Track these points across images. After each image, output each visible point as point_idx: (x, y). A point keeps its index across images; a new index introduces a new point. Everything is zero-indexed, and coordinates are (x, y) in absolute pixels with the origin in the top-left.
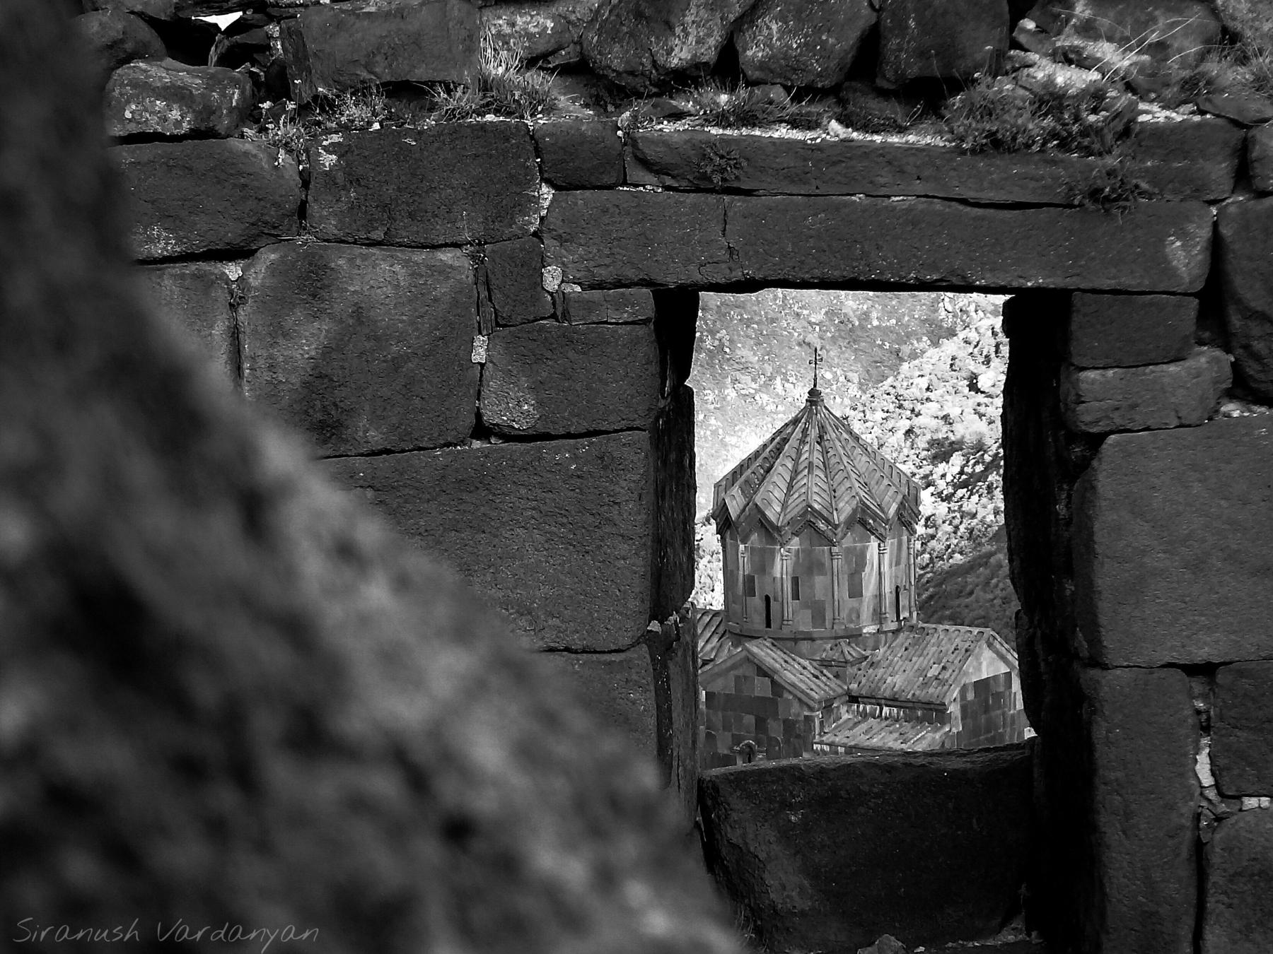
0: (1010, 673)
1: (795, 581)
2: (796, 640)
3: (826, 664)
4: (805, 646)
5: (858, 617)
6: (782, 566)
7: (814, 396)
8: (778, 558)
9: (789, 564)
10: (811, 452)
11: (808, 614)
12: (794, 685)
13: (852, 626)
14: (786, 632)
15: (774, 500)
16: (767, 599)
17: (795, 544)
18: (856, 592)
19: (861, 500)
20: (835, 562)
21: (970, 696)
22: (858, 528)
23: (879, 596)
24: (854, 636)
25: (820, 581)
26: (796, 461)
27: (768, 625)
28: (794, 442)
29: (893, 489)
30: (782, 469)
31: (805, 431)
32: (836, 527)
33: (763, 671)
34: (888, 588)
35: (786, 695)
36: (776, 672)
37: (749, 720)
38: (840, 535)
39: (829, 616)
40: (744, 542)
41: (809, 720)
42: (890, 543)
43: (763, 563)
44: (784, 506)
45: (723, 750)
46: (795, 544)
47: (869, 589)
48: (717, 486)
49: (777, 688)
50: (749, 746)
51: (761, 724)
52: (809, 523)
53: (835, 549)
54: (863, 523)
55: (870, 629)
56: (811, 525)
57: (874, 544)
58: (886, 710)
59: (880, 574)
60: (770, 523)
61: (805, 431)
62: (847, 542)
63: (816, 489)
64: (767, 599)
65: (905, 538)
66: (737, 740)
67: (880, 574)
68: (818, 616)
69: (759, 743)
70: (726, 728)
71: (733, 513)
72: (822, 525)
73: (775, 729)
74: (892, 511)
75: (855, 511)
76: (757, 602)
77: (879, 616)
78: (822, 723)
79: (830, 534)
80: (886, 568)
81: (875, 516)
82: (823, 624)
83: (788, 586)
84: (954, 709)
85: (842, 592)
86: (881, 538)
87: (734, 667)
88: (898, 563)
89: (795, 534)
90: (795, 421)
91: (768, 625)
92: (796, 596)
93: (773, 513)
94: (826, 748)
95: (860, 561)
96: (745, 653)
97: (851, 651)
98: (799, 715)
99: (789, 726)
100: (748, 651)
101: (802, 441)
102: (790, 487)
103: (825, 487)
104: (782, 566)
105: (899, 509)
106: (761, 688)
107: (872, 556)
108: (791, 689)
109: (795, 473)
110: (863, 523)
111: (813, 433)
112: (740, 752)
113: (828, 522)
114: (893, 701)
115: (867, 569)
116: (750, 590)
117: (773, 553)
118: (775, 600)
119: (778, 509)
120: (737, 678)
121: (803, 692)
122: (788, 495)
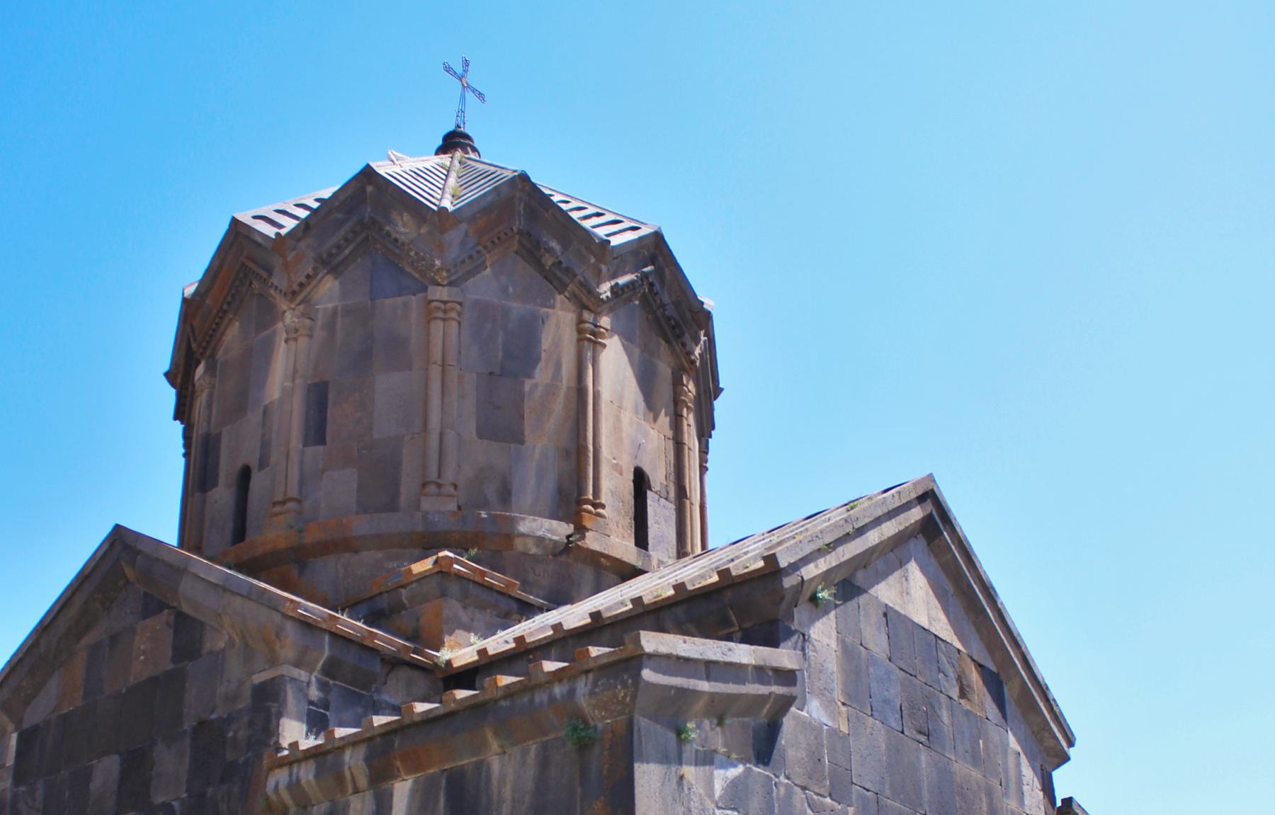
5: (505, 495)
16: (245, 475)
17: (328, 291)
18: (502, 425)
20: (437, 327)
25: (387, 385)
39: (407, 487)
62: (483, 287)
67: (581, 391)
68: (381, 484)
72: (403, 227)
76: (222, 495)
83: (297, 406)
85: (453, 410)
89: (331, 264)
92: (316, 432)
98: (232, 698)
107: (557, 344)
115: (542, 375)
118: (263, 463)
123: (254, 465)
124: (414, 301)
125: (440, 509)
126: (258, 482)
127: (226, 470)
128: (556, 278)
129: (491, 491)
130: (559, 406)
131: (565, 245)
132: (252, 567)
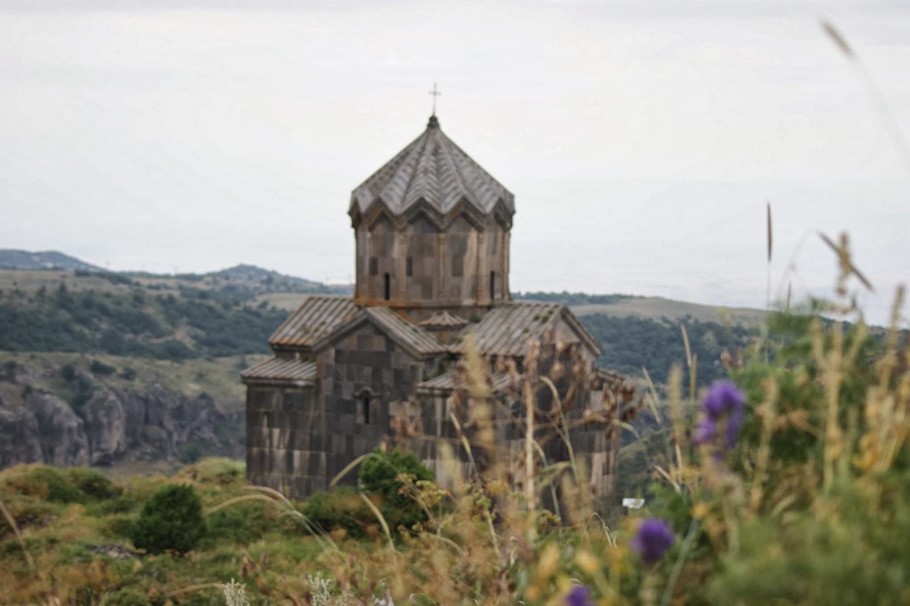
0: (578, 345)
1: (410, 262)
3: (429, 328)
4: (414, 314)
5: (459, 292)
6: (398, 250)
7: (433, 123)
9: (405, 248)
10: (428, 160)
11: (417, 289)
12: (402, 340)
13: (453, 299)
14: (400, 302)
16: (387, 277)
17: (411, 231)
18: (458, 271)
22: (462, 221)
23: (477, 277)
25: (429, 261)
26: (415, 169)
27: (387, 297)
28: (414, 155)
29: (489, 194)
30: (402, 177)
32: (442, 216)
33: (380, 331)
34: (485, 271)
35: (398, 350)
36: (389, 330)
37: (368, 370)
38: (446, 224)
40: (371, 229)
41: (414, 368)
42: (487, 236)
44: (403, 199)
45: (347, 396)
47: (469, 270)
48: (354, 192)
49: (391, 343)
50: (366, 392)
51: (376, 373)
52: (421, 214)
53: (442, 236)
54: (465, 216)
55: (468, 302)
56: (422, 215)
57: (473, 235)
59: (478, 259)
60: (390, 212)
61: (423, 149)
62: (453, 231)
63: (428, 187)
64: (387, 277)
65: (500, 234)
66: (357, 387)
67: (478, 259)
69: (374, 388)
70: (350, 378)
71: (364, 207)
72: (431, 215)
73: (387, 377)
74: (489, 208)
75: (458, 205)
76: (380, 279)
77: (475, 292)
78: (425, 372)
79: (437, 222)
80: (483, 254)
81: (476, 211)
82: (430, 297)
83: (403, 265)
86: (480, 230)
88: (494, 252)
89: (411, 222)
90: (416, 142)
91: (387, 297)
92: (409, 272)
93: (396, 204)
94: (427, 391)
96: (364, 317)
99: (398, 374)
100: (366, 313)
101: (421, 154)
102: (409, 186)
103: (435, 186)
104: (398, 250)
105: (495, 208)
106: (378, 344)
108: (399, 342)
109: (413, 177)
110: (465, 216)
111: (430, 147)
112: (360, 398)
113: (437, 213)
116: (374, 270)
117: (392, 239)
118: (394, 276)
120: (360, 337)
121: (410, 345)
122: (406, 192)
123: (390, 273)
124: (434, 235)
125: (444, 301)
126: (392, 282)
127: (381, 271)
128: (472, 223)
129: (456, 292)
131: (475, 214)
132: (394, 309)
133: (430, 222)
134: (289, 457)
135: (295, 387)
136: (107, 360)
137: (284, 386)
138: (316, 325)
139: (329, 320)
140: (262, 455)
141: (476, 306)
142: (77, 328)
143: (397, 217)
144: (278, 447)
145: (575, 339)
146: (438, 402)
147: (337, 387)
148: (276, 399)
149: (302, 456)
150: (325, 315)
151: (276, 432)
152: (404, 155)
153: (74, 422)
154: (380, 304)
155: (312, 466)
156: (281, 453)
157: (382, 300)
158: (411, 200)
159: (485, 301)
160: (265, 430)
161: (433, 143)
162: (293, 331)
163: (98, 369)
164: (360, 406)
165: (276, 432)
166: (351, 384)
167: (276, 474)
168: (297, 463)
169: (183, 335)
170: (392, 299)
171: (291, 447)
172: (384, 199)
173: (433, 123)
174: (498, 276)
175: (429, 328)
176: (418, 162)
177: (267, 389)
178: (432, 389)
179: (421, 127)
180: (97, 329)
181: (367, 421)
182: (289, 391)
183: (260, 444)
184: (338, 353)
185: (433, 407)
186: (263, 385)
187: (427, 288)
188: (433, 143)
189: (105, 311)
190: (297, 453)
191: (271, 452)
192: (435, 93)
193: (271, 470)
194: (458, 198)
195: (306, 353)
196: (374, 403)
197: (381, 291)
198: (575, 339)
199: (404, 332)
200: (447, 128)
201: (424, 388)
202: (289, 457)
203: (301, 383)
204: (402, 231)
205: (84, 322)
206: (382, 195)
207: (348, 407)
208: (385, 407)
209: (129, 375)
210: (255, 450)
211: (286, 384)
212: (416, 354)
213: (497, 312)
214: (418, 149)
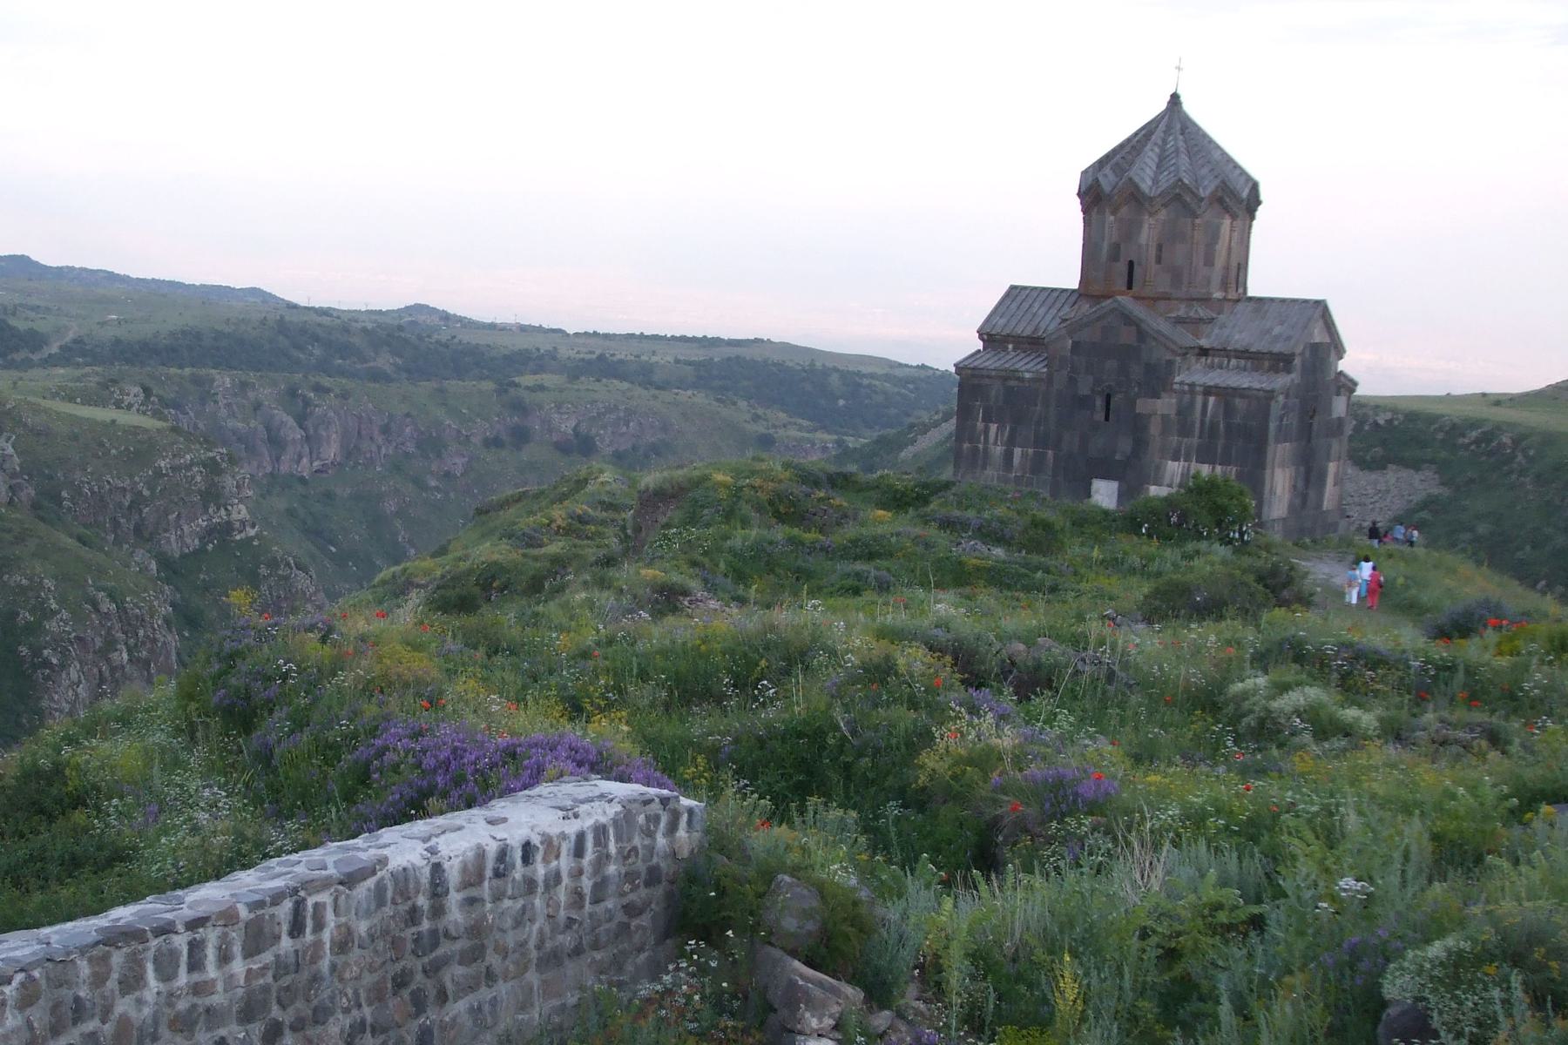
1: (1160, 248)
2: (1155, 299)
3: (1179, 321)
4: (1162, 305)
5: (1209, 282)
6: (1148, 233)
7: (1175, 99)
8: (1146, 226)
10: (1176, 139)
12: (1159, 332)
15: (1145, 176)
16: (1131, 264)
17: (1163, 215)
18: (1209, 261)
19: (1223, 182)
21: (1307, 354)
23: (1227, 268)
24: (1206, 300)
27: (1130, 287)
30: (1150, 156)
31: (1169, 128)
33: (1128, 319)
34: (1234, 264)
37: (1111, 364)
40: (1114, 213)
41: (1170, 363)
42: (1238, 223)
43: (1129, 231)
44: (1155, 181)
45: (1084, 390)
46: (1163, 215)
47: (1220, 262)
48: (1084, 173)
49: (1142, 335)
52: (1180, 199)
54: (1220, 201)
55: (1218, 295)
56: (1178, 197)
57: (1227, 222)
58: (1233, 362)
59: (1230, 249)
64: (1131, 264)
67: (1230, 249)
71: (1107, 188)
74: (1245, 194)
76: (1122, 267)
79: (1193, 206)
81: (1234, 194)
83: (1153, 252)
84: (1297, 361)
86: (1234, 217)
87: (1099, 319)
89: (1165, 205)
91: (1130, 287)
92: (1159, 260)
93: (1146, 186)
95: (1214, 237)
97: (1202, 312)
102: (1158, 167)
104: (1148, 233)
106: (1127, 336)
110: (1220, 201)
113: (1195, 195)
114: (1244, 354)
119: (1150, 183)
126: (1137, 270)
128: (1227, 210)
130: (1224, 253)
132: (1136, 298)
133: (1185, 205)
134: (1008, 456)
135: (1021, 379)
136: (326, 381)
137: (1006, 379)
138: (1029, 316)
139: (1043, 310)
140: (975, 451)
141: (1225, 299)
142: (296, 353)
143: (1151, 199)
144: (995, 443)
145: (1328, 340)
146: (1199, 399)
147: (1072, 380)
148: (996, 390)
149: (1024, 455)
150: (1036, 305)
151: (993, 427)
152: (1147, 132)
153: (298, 434)
154: (1122, 294)
155: (1037, 465)
156: (998, 450)
157: (1124, 288)
158: (1166, 181)
159: (1232, 295)
160: (980, 425)
161: (1173, 127)
162: (1003, 321)
163: (318, 388)
164: (1099, 402)
165: (993, 427)
166: (1091, 378)
167: (989, 472)
168: (1016, 460)
169: (384, 361)
170: (1135, 288)
171: (1011, 443)
172: (1136, 179)
173: (1175, 99)
174: (1242, 267)
175: (1179, 321)
176: (1165, 141)
177: (987, 381)
178: (1192, 385)
179: (1163, 106)
180: (311, 354)
181: (1107, 419)
182: (1012, 383)
183: (973, 439)
184: (1076, 345)
185: (1192, 404)
186: (982, 376)
187: (1176, 276)
188: (1173, 127)
189: (316, 338)
190: (1018, 451)
191: (986, 449)
192: (1179, 68)
193: (984, 467)
194: (1217, 182)
195: (1031, 344)
196: (1115, 399)
197: (1121, 283)
198: (1328, 340)
199: (1158, 323)
200: (1190, 107)
201: (1182, 383)
202: (1008, 456)
203: (1027, 375)
204: (1151, 215)
205: (300, 348)
206: (1132, 174)
207: (1084, 402)
208: (1133, 404)
209: (345, 396)
210: (966, 445)
211: (1011, 375)
212: (1173, 347)
213: (1240, 306)
214: (1162, 126)
